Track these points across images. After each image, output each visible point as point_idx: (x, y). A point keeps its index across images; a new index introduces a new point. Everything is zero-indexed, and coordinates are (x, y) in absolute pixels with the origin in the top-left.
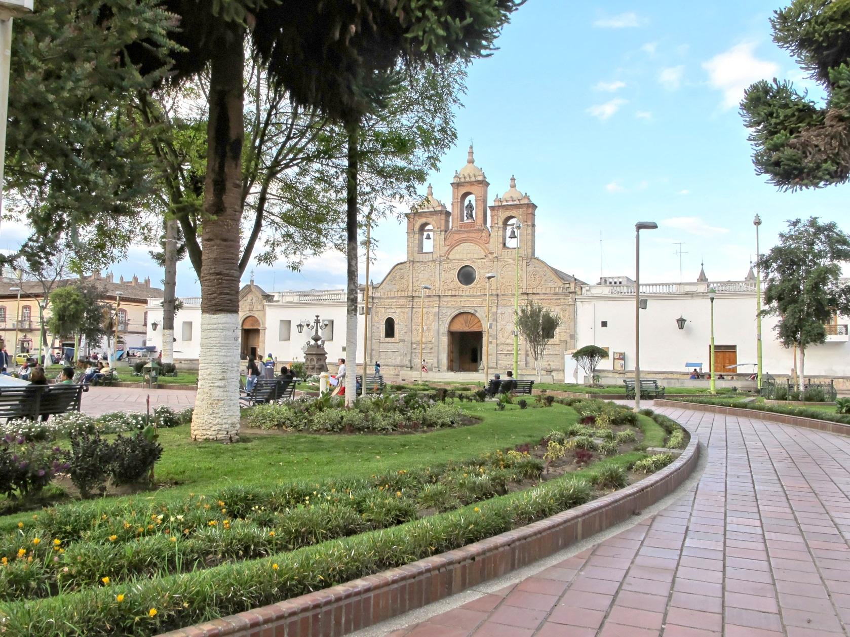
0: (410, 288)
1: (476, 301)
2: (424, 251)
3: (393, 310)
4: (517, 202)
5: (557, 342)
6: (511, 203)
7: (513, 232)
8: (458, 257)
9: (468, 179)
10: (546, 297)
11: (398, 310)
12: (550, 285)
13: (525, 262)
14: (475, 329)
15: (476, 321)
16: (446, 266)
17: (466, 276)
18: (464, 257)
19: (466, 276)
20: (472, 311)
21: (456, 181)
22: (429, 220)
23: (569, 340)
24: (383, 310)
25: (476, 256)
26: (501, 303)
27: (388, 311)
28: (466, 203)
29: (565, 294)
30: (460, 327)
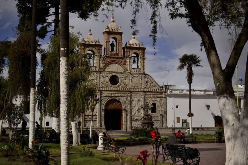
1: (120, 94)
4: (138, 46)
5: (158, 115)
6: (135, 46)
8: (109, 70)
9: (114, 31)
10: (153, 93)
12: (154, 88)
13: (143, 76)
14: (119, 108)
16: (103, 74)
17: (114, 80)
18: (113, 71)
19: (114, 80)
20: (118, 99)
22: (93, 49)
23: (164, 114)
25: (119, 71)
26: (133, 95)
28: (111, 42)
30: (111, 107)
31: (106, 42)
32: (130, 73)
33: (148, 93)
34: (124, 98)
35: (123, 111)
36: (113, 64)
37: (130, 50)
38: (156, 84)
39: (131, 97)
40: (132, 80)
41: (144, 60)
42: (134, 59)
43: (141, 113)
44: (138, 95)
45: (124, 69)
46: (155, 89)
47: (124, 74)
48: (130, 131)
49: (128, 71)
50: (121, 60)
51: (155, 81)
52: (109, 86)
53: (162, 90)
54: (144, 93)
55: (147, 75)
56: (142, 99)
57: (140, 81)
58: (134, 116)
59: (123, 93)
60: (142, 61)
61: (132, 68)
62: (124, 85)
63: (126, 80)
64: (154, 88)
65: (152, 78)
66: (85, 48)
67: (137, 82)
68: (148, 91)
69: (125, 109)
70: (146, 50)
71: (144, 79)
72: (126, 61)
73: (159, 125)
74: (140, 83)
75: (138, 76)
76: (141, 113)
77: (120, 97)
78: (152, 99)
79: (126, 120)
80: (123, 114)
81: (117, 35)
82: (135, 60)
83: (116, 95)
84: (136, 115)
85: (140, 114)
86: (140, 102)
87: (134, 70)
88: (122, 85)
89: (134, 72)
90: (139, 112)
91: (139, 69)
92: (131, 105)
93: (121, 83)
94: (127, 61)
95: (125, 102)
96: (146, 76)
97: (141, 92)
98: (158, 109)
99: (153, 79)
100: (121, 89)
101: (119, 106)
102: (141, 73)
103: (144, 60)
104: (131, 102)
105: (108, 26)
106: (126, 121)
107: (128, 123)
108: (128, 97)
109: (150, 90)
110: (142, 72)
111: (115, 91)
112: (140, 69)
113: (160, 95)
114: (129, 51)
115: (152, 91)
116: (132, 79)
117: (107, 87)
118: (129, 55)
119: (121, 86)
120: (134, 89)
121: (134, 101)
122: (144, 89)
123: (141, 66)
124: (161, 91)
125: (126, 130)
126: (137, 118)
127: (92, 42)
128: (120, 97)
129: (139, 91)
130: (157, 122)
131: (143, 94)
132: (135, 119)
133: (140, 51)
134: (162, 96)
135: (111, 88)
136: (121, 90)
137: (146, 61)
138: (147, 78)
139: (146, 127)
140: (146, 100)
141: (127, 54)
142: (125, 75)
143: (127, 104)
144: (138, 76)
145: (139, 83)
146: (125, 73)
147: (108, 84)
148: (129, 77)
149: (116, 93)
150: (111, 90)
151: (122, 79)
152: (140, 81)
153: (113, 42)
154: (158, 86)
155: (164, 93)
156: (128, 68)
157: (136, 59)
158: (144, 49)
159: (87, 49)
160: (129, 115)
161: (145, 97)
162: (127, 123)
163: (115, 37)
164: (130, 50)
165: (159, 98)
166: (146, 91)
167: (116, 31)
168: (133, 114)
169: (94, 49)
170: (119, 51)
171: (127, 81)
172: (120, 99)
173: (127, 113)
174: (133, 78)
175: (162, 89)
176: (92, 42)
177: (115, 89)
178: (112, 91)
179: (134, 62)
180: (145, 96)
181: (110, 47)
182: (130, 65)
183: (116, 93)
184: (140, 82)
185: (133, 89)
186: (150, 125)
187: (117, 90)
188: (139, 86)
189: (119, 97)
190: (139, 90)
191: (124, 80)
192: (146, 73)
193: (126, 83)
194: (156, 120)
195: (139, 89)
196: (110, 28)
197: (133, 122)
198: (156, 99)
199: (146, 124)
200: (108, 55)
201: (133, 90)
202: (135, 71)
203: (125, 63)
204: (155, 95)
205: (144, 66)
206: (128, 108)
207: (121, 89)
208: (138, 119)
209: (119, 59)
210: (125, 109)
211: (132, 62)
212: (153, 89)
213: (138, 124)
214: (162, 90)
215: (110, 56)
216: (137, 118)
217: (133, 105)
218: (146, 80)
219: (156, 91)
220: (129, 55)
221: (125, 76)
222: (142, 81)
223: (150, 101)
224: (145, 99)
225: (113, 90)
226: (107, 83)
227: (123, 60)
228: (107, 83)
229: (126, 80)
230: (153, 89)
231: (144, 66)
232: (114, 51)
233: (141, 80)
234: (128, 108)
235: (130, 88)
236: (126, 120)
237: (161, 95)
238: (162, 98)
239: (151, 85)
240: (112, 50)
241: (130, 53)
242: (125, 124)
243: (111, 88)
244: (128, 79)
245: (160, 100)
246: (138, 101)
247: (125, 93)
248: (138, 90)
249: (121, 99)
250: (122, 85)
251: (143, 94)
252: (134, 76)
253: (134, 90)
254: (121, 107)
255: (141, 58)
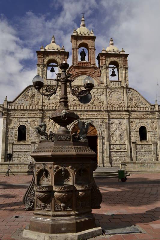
0: (40, 103)
2: (47, 78)
3: (25, 120)
5: (150, 143)
7: (113, 72)
9: (83, 35)
11: (30, 120)
12: (142, 106)
13: (125, 91)
15: (93, 128)
21: (75, 34)
22: (55, 58)
24: (16, 119)
26: (112, 116)
27: (21, 120)
29: (152, 112)
31: (73, 49)
32: (107, 87)
33: (134, 113)
34: (99, 119)
35: (98, 138)
36: (83, 76)
37: (106, 58)
38: (144, 101)
39: (109, 119)
40: (110, 96)
41: (125, 71)
42: (113, 70)
43: (124, 140)
44: (119, 116)
45: (98, 82)
46: (143, 108)
47: (99, 88)
48: (109, 167)
49: (104, 85)
50: (94, 71)
51: (142, 97)
52: (77, 104)
53: (154, 108)
54: (128, 113)
55: (131, 90)
56: (125, 121)
57: (121, 97)
58: (114, 145)
59: (96, 113)
60: (124, 72)
61: (110, 81)
62: (99, 104)
63: (101, 96)
64: (141, 107)
65: (139, 93)
66: (44, 57)
67: (117, 98)
68: (133, 110)
69: (101, 135)
70: (128, 57)
71: (127, 94)
72: (101, 72)
73: (151, 157)
74: (122, 100)
75: (118, 90)
76: (124, 140)
77: (94, 118)
78: (140, 121)
79: (103, 150)
80: (99, 142)
81: (87, 40)
82: (114, 71)
83: (87, 116)
84: (117, 143)
85: (123, 141)
86: (123, 125)
87: (112, 84)
88: (96, 103)
89: (112, 85)
90: (122, 139)
91: (120, 81)
92: (109, 129)
93: (94, 100)
94: (102, 71)
95: (101, 125)
96: (129, 90)
97: (124, 111)
98: (149, 135)
99: (140, 95)
100: (94, 108)
101: (92, 132)
102: (123, 87)
103: (125, 71)
104: (109, 127)
105: (77, 31)
106: (103, 152)
107: (106, 155)
108: (104, 119)
109: (136, 109)
110: (124, 85)
111: (85, 111)
112: (121, 82)
113: (151, 116)
114: (105, 59)
115: (139, 109)
116: (109, 95)
117: (74, 106)
118: (105, 64)
119: (94, 104)
120: (114, 108)
121: (114, 125)
122: (127, 108)
123: (123, 78)
124: (152, 110)
125: (102, 165)
126: (118, 147)
127: (54, 50)
128: (94, 118)
129: (121, 110)
130: (148, 152)
131: (126, 114)
132: (116, 148)
133: (121, 59)
134: (154, 116)
135: (80, 108)
136: (94, 109)
137: (128, 71)
138: (131, 93)
139: (51, 177)
140: (131, 122)
141: (102, 62)
142: (100, 90)
143: (104, 128)
144: (118, 90)
145: (120, 100)
146: (99, 87)
147: (76, 101)
148: (105, 92)
149: (87, 114)
150: (80, 109)
151: (96, 95)
152: (121, 97)
153: (83, 50)
154: (147, 104)
155: (156, 113)
156: (105, 81)
157: (116, 70)
158: (126, 56)
159: (47, 59)
160: (107, 143)
161: (129, 119)
162: (104, 154)
163: (85, 42)
164: (106, 58)
165: (150, 119)
166: (130, 109)
167: (87, 35)
168: (113, 142)
169: (57, 57)
170: (90, 59)
171: (103, 98)
172: (93, 122)
173: (104, 141)
174: (111, 94)
175: (154, 107)
176: (54, 50)
177: (86, 108)
178: (81, 111)
179: (113, 75)
180: (129, 117)
181: (79, 57)
182: (107, 77)
183: (87, 114)
184: (122, 99)
185: (111, 108)
186: (69, 168)
187: (88, 109)
188: (120, 104)
189: (91, 118)
190: (120, 109)
191: (98, 96)
192: (129, 86)
193: (102, 101)
194: (147, 150)
195: (121, 108)
196: (78, 33)
197: (113, 154)
198: (146, 121)
199: (49, 166)
200: (75, 65)
201: (111, 110)
202: (115, 84)
203: (99, 74)
204: (144, 115)
205: (126, 77)
206: (106, 134)
207: (94, 108)
208: (120, 149)
209: (91, 70)
210: (101, 135)
211: (111, 73)
212: (140, 108)
213: (121, 156)
214: (154, 108)
215: (78, 66)
216: (118, 147)
217: (112, 130)
218: (130, 95)
219: (144, 110)
220: (105, 64)
221: (99, 91)
222: (124, 97)
223: (136, 126)
224: (129, 122)
225: (83, 109)
226: (74, 100)
227: (96, 71)
228: (74, 100)
229: (102, 97)
230: (140, 108)
231: (126, 77)
232: (85, 60)
233: (122, 96)
234: (106, 134)
235: (107, 107)
236: (103, 150)
237: (152, 115)
238: (155, 120)
239: (137, 103)
240: (83, 58)
241: (106, 62)
242: (102, 156)
243: (80, 108)
244: (105, 94)
245: (152, 122)
246: (119, 123)
247: (100, 113)
248: (119, 110)
249: (95, 121)
250: (96, 103)
251: (126, 114)
252: (113, 90)
253: (114, 109)
254: (96, 132)
255: (121, 68)
